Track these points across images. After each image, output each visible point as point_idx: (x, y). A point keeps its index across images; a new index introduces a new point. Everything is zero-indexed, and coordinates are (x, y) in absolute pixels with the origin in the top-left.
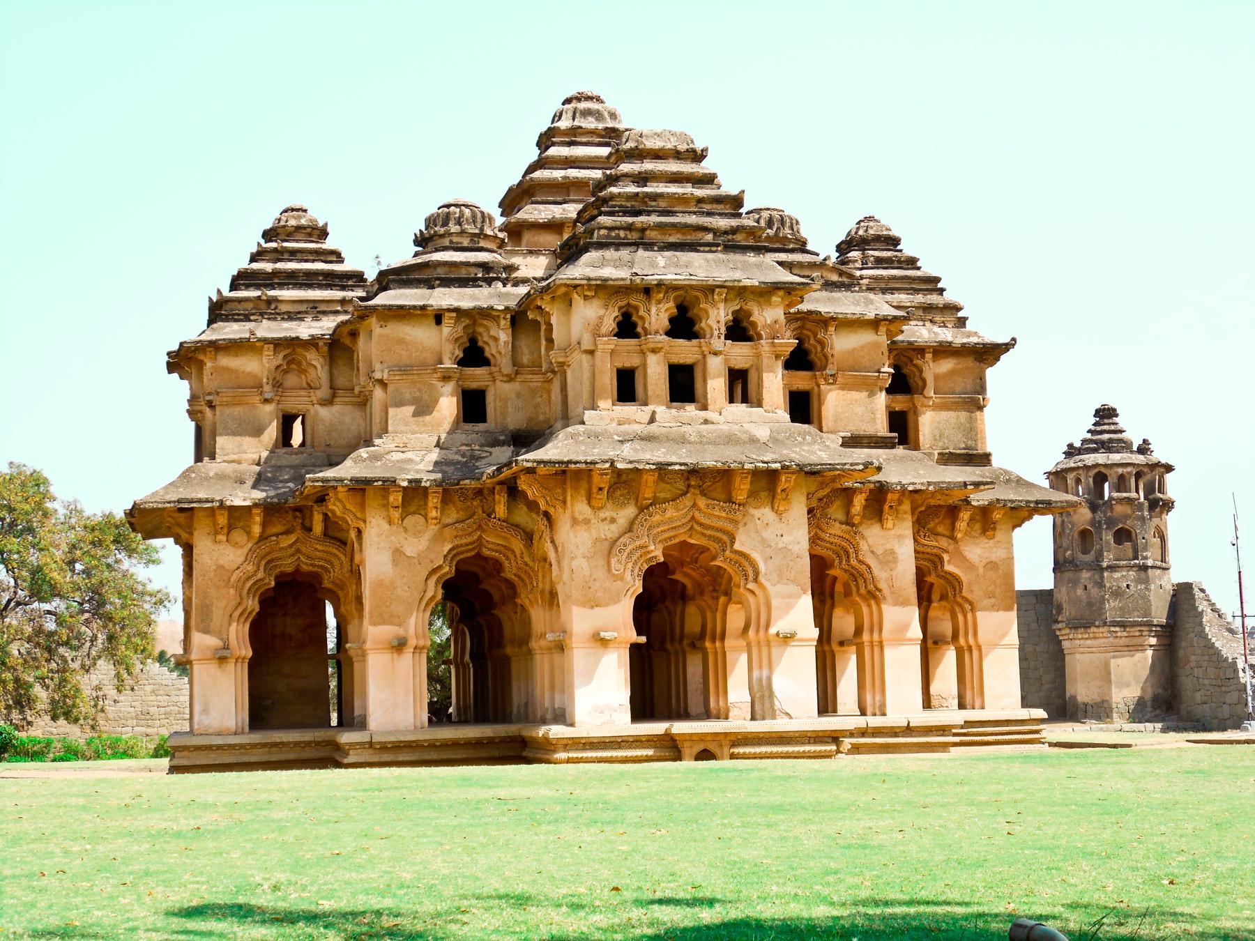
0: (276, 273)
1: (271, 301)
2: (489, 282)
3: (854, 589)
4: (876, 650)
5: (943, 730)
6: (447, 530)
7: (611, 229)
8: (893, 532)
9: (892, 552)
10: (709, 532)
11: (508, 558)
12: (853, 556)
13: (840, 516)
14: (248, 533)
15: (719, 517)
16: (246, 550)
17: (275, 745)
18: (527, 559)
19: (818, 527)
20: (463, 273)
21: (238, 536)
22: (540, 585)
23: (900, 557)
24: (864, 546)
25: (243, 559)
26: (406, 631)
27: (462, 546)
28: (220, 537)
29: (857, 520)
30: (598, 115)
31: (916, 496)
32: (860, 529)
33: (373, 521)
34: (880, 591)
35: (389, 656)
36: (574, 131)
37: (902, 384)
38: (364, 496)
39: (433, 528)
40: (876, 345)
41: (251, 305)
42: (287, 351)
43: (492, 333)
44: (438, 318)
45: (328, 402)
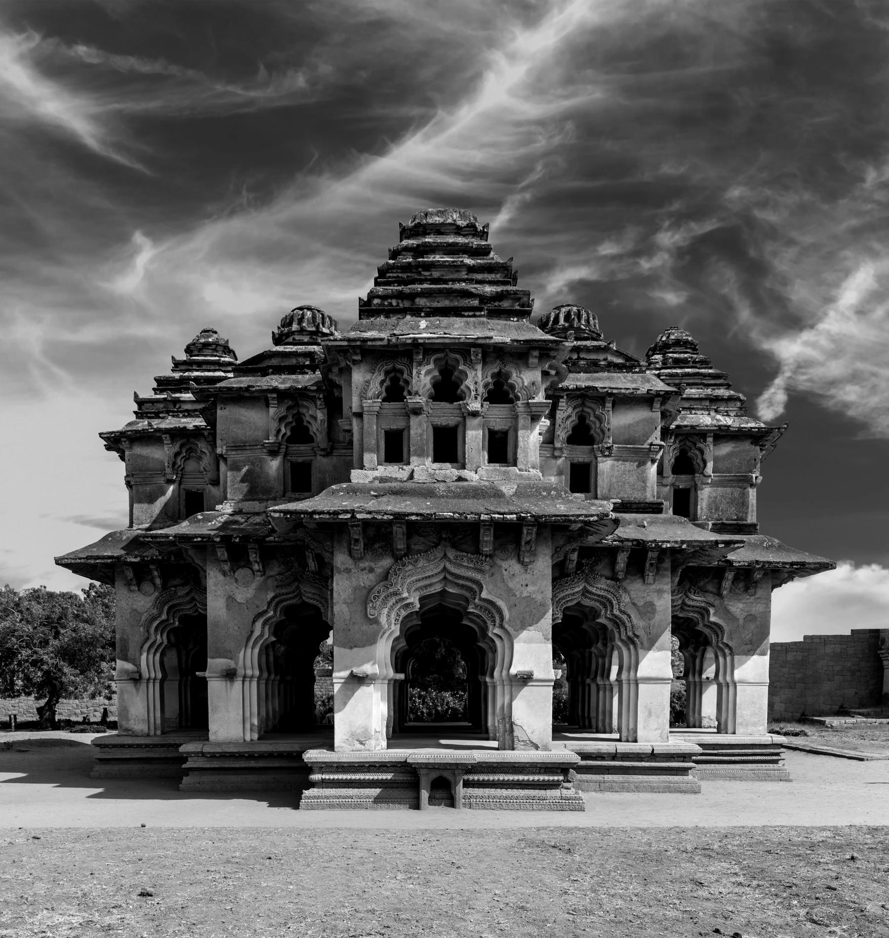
3: (617, 635)
4: (632, 687)
5: (684, 757)
8: (654, 586)
9: (651, 604)
12: (616, 606)
13: (607, 573)
19: (587, 581)
23: (658, 609)
24: (626, 599)
27: (283, 594)
29: (621, 576)
31: (679, 556)
32: (624, 584)
33: (212, 573)
34: (637, 637)
35: (224, 683)
37: (686, 465)
39: (259, 579)
40: (651, 421)
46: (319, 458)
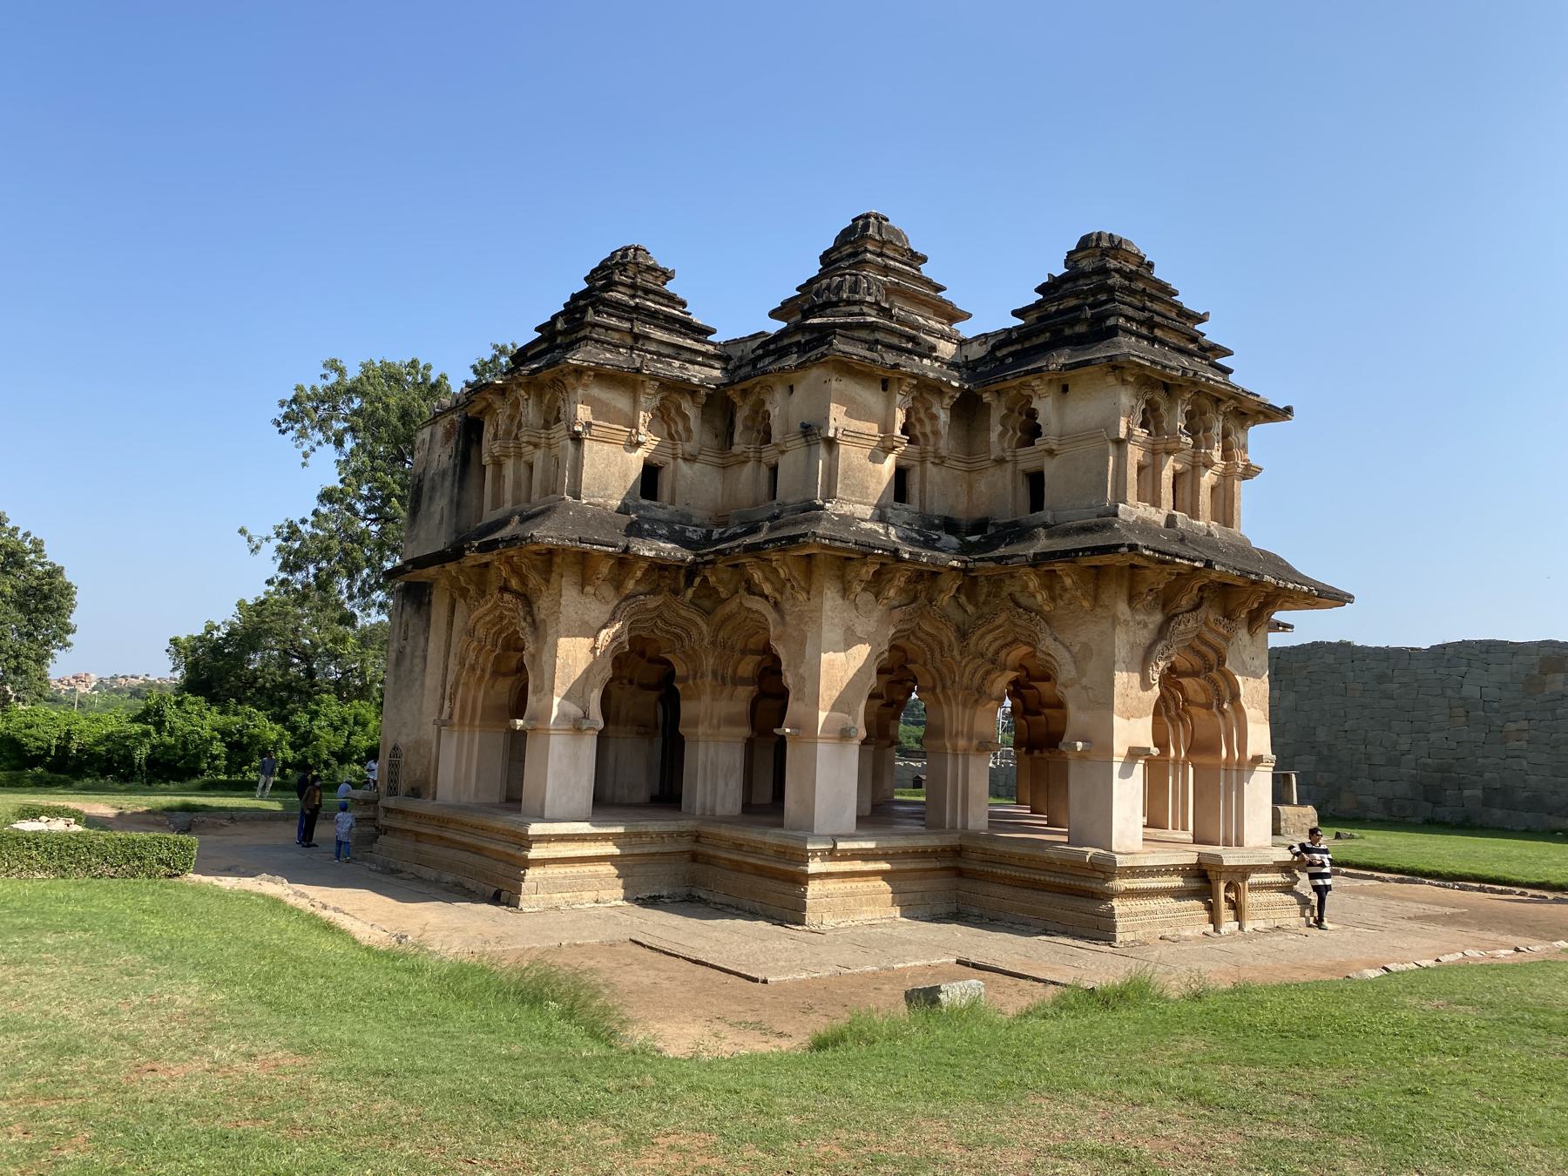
0: (637, 308)
1: (636, 337)
2: (922, 356)
6: (897, 614)
7: (1128, 319)
10: (1204, 648)
11: (932, 651)
14: (618, 586)
15: (1219, 634)
16: (611, 607)
17: (639, 835)
18: (956, 653)
20: (895, 341)
21: (608, 591)
22: (965, 681)
25: (607, 616)
26: (855, 721)
28: (589, 589)
30: (898, 234)
36: (884, 243)
38: (809, 563)
41: (617, 335)
42: (665, 394)
43: (934, 410)
44: (885, 385)
45: (690, 459)
46: (929, 465)
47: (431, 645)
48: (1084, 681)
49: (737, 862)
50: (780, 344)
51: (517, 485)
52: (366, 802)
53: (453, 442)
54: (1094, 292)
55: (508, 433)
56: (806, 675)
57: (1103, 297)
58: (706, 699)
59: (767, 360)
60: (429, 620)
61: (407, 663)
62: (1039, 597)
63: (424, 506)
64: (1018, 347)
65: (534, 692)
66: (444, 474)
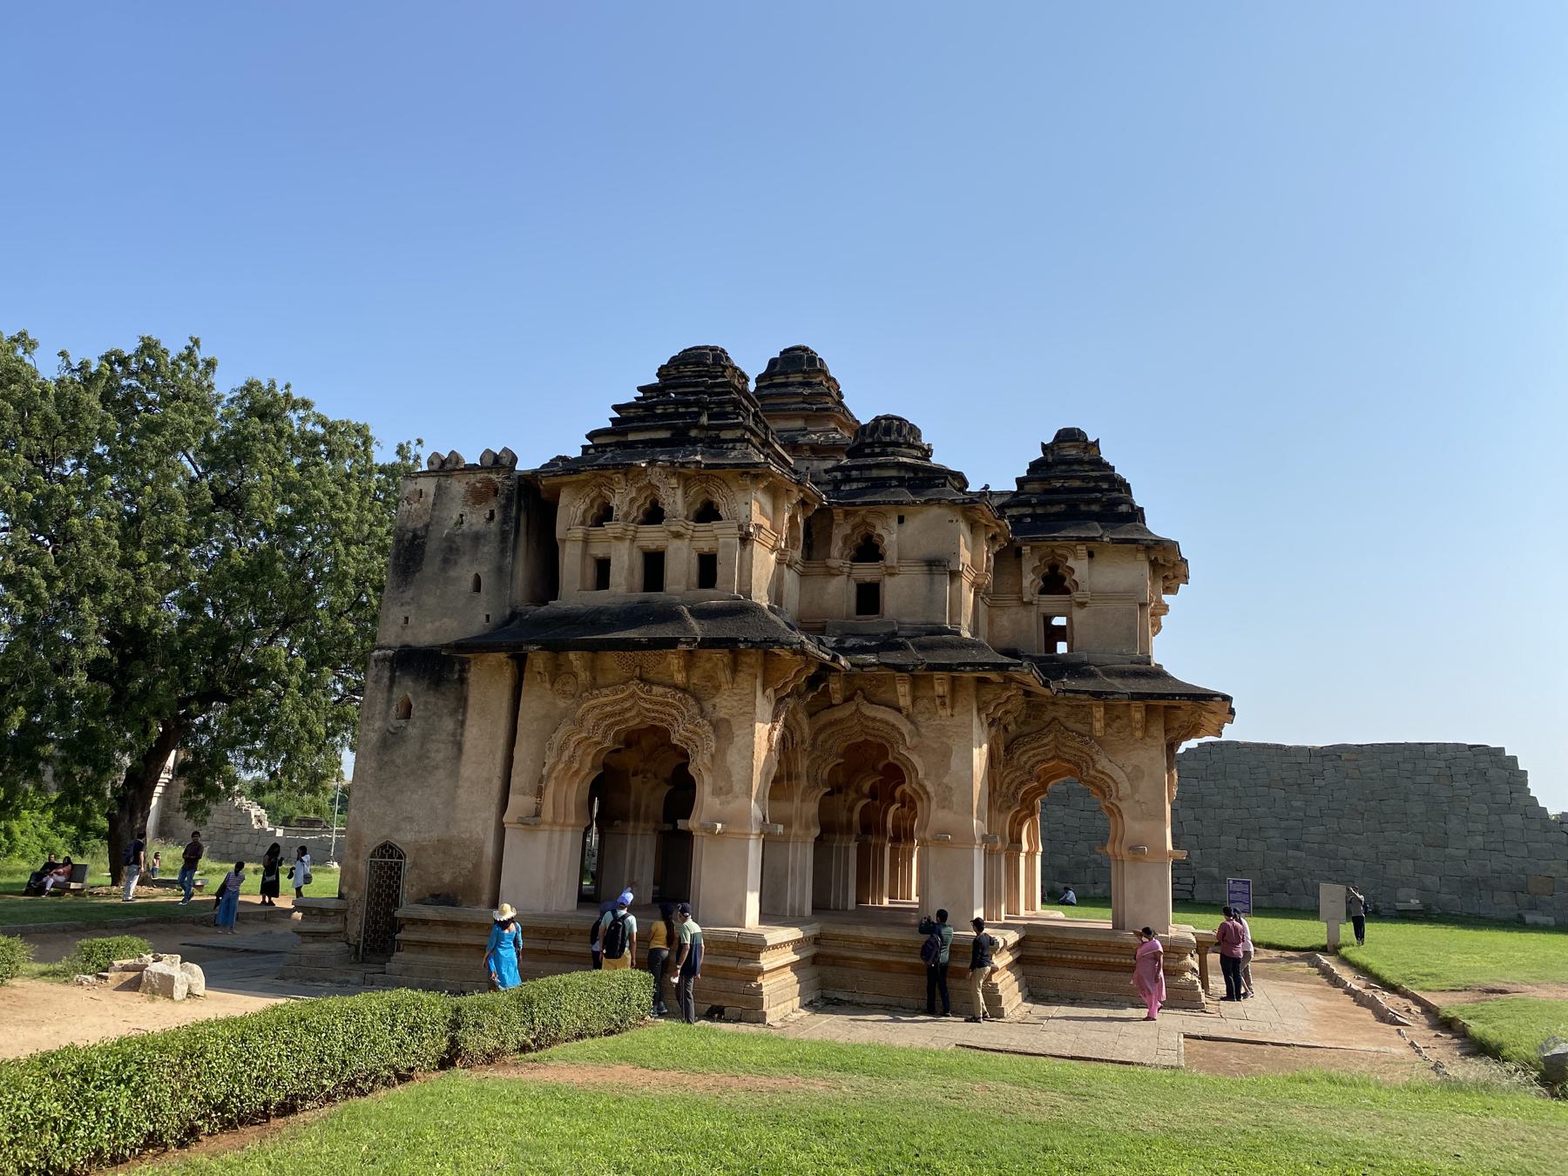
6: (994, 729)
28: (769, 691)
47: (472, 733)
48: (1137, 797)
49: (883, 962)
50: (867, 474)
51: (631, 570)
52: (337, 912)
53: (494, 504)
54: (1097, 479)
55: (626, 515)
56: (954, 785)
57: (1105, 486)
58: (797, 801)
59: (854, 486)
60: (462, 702)
61: (410, 748)
62: (1098, 725)
63: (430, 567)
64: (1028, 511)
65: (717, 792)
66: (477, 538)
